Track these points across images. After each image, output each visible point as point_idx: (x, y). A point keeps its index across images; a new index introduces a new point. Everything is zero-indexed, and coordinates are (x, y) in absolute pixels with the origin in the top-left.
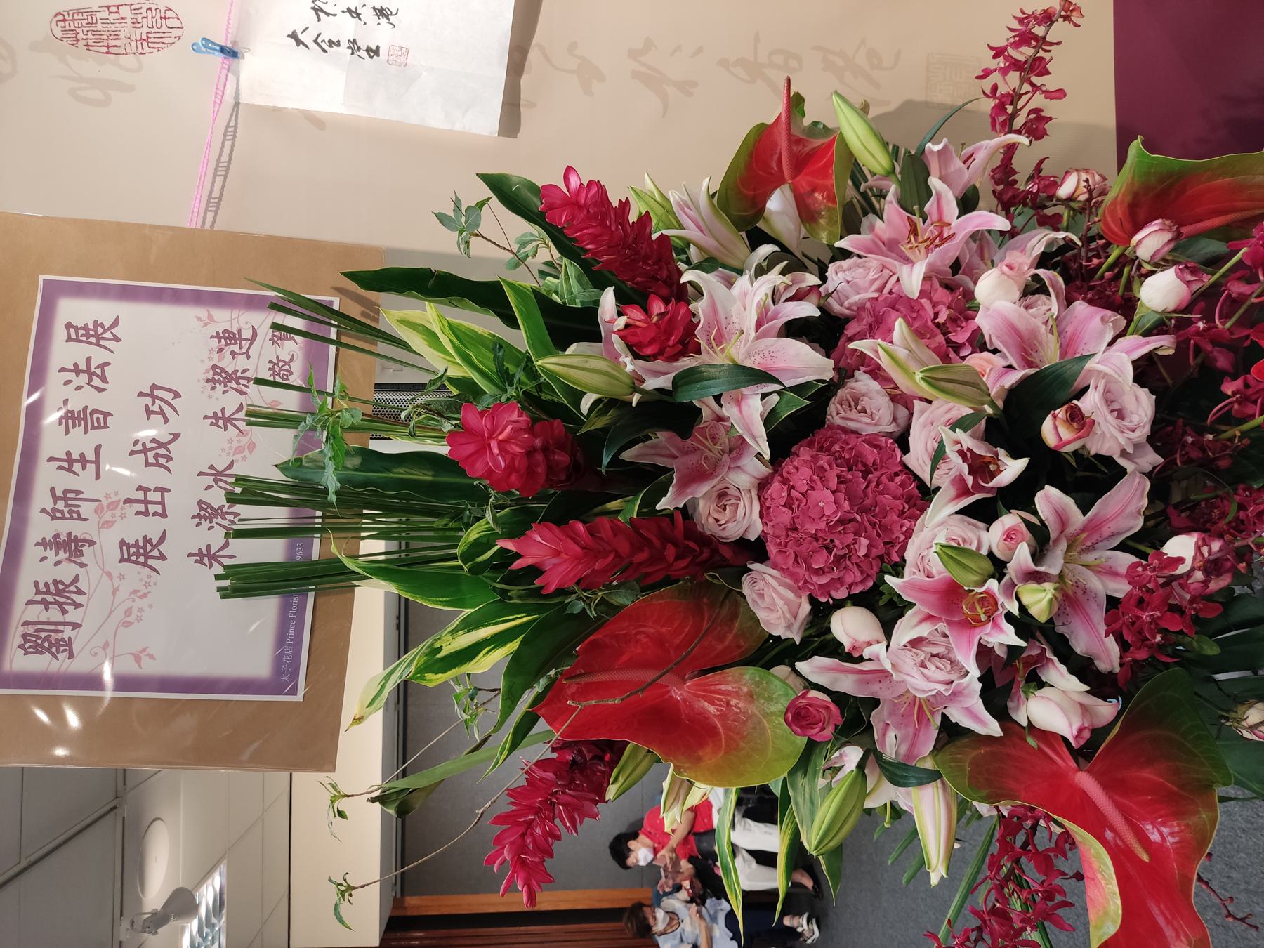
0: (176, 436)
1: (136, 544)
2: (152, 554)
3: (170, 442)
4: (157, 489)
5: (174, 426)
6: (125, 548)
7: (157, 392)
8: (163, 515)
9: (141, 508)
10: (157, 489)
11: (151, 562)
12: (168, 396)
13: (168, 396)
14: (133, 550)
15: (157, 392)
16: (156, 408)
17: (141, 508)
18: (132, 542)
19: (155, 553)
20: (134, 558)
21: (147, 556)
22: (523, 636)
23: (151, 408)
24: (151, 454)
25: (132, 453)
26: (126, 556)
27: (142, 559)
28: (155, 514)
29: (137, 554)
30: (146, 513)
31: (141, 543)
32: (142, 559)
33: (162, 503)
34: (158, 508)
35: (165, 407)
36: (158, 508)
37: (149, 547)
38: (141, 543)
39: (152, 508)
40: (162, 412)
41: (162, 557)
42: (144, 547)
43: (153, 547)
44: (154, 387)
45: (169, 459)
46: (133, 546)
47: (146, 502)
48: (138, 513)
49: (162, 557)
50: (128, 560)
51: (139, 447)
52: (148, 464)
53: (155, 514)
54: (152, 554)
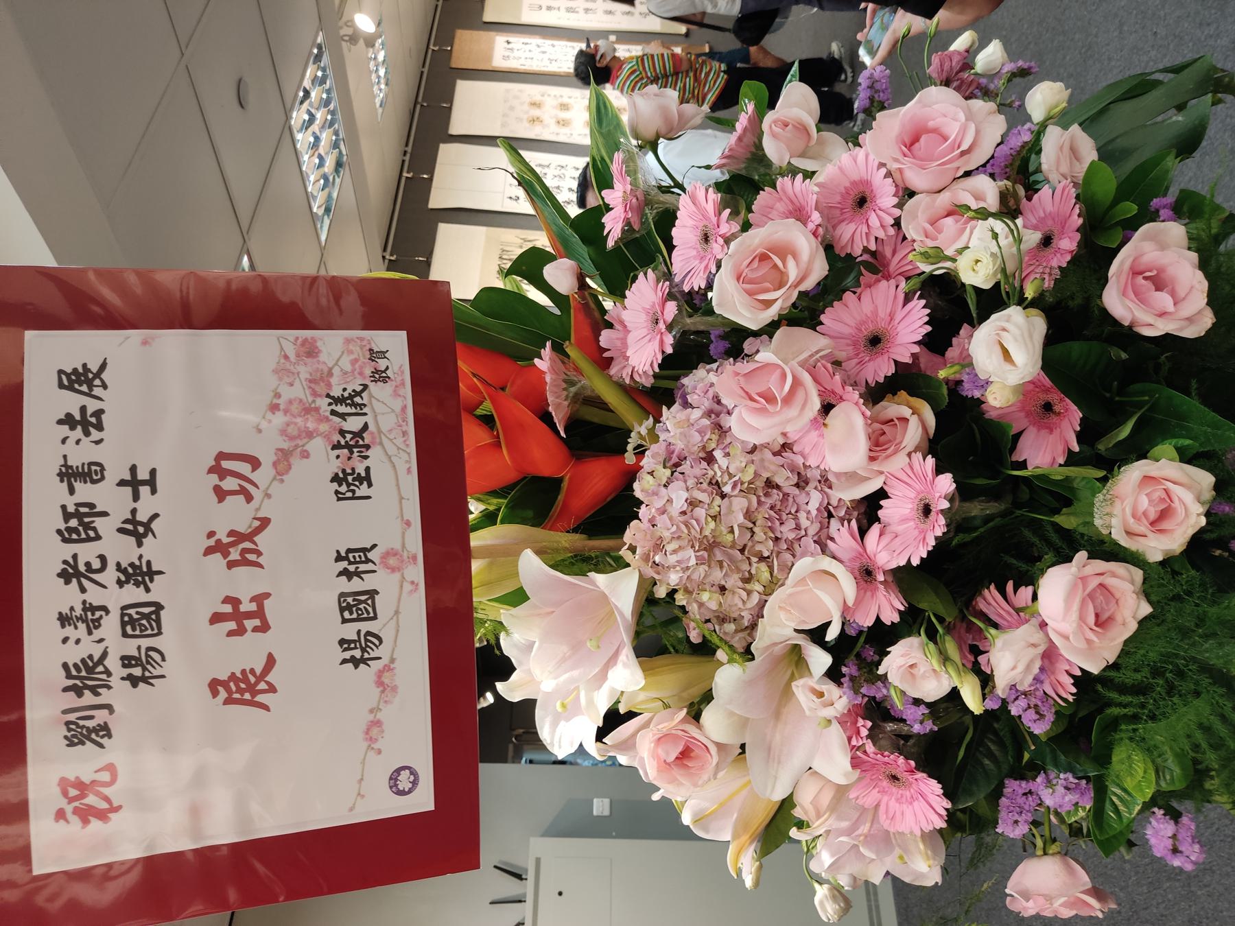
2: (259, 687)
7: (226, 464)
9: (232, 625)
12: (244, 468)
15: (226, 464)
16: (230, 484)
17: (232, 625)
21: (255, 693)
22: (958, 761)
27: (247, 696)
28: (255, 629)
29: (241, 691)
30: (240, 631)
34: (257, 622)
36: (257, 622)
39: (249, 624)
43: (260, 678)
44: (221, 456)
45: (259, 554)
48: (231, 634)
49: (272, 689)
54: (259, 687)
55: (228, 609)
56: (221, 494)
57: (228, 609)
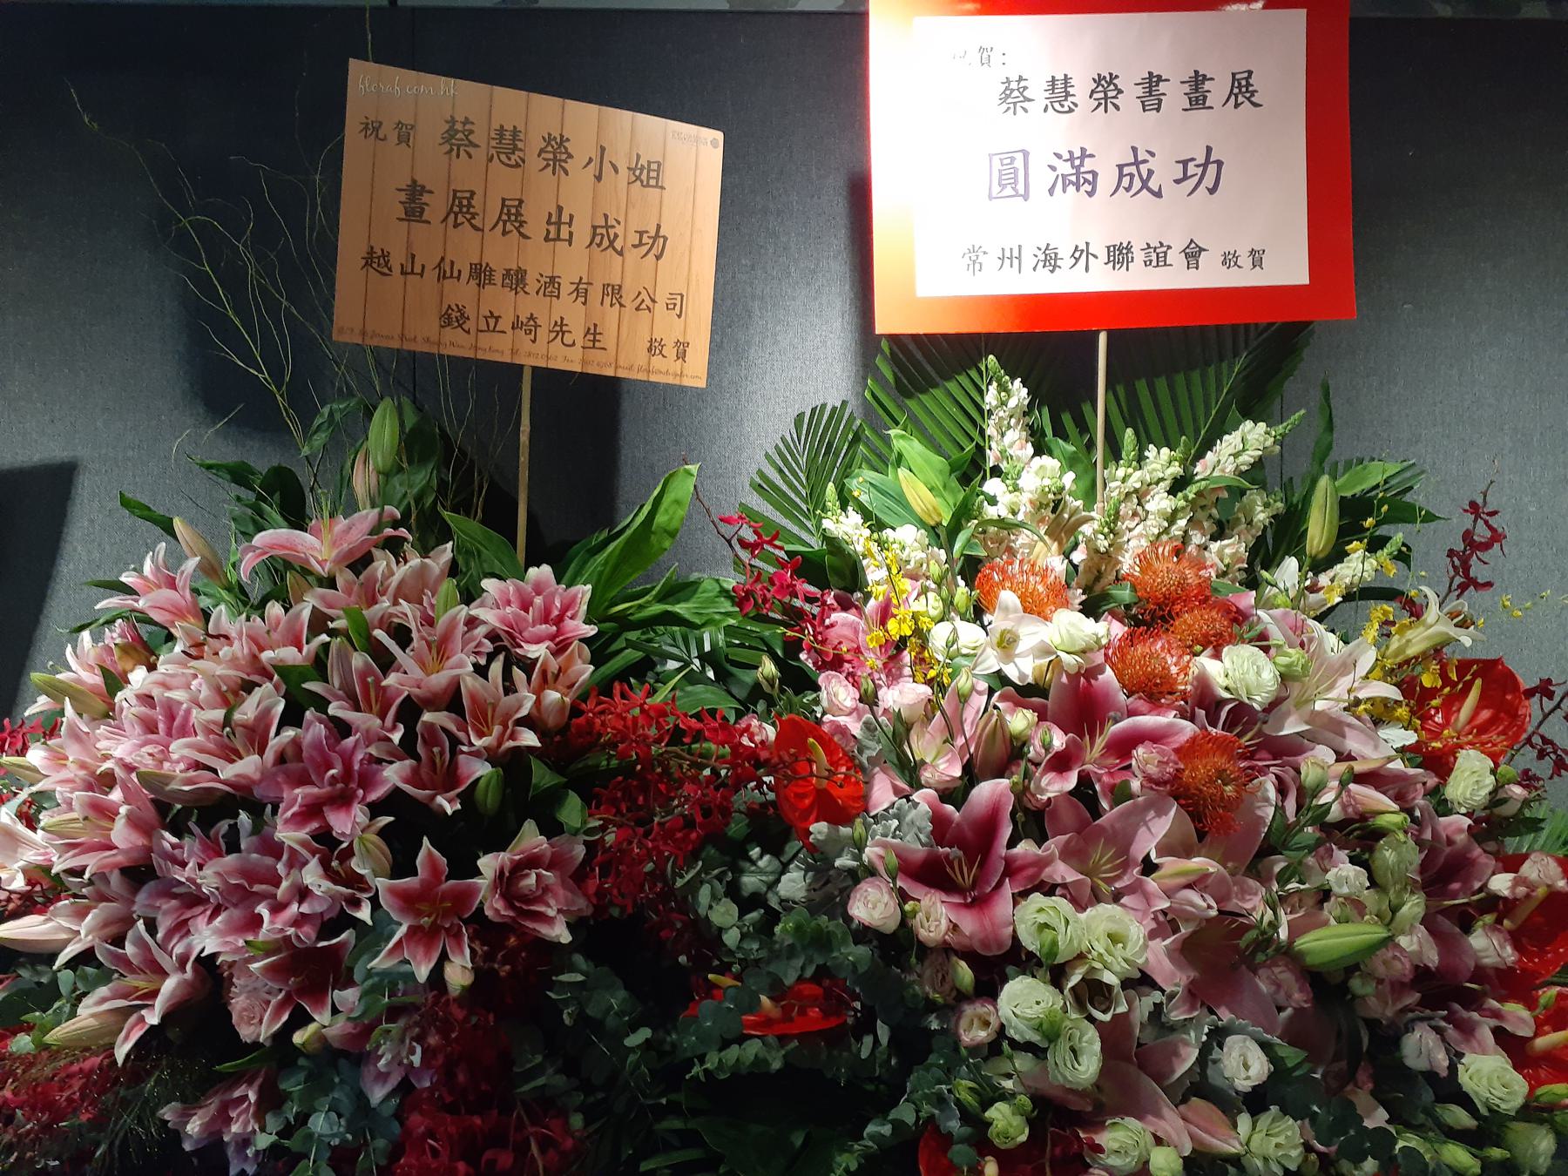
0: (620, 253)
1: (518, 214)
3: (614, 249)
4: (571, 234)
8: (547, 239)
9: (553, 219)
10: (571, 234)
20: (505, 210)
23: (645, 236)
28: (548, 232)
30: (549, 223)
32: (505, 217)
39: (552, 229)
40: (641, 244)
47: (559, 223)
48: (550, 215)
50: (503, 205)
51: (611, 222)
53: (548, 232)
57: (565, 218)
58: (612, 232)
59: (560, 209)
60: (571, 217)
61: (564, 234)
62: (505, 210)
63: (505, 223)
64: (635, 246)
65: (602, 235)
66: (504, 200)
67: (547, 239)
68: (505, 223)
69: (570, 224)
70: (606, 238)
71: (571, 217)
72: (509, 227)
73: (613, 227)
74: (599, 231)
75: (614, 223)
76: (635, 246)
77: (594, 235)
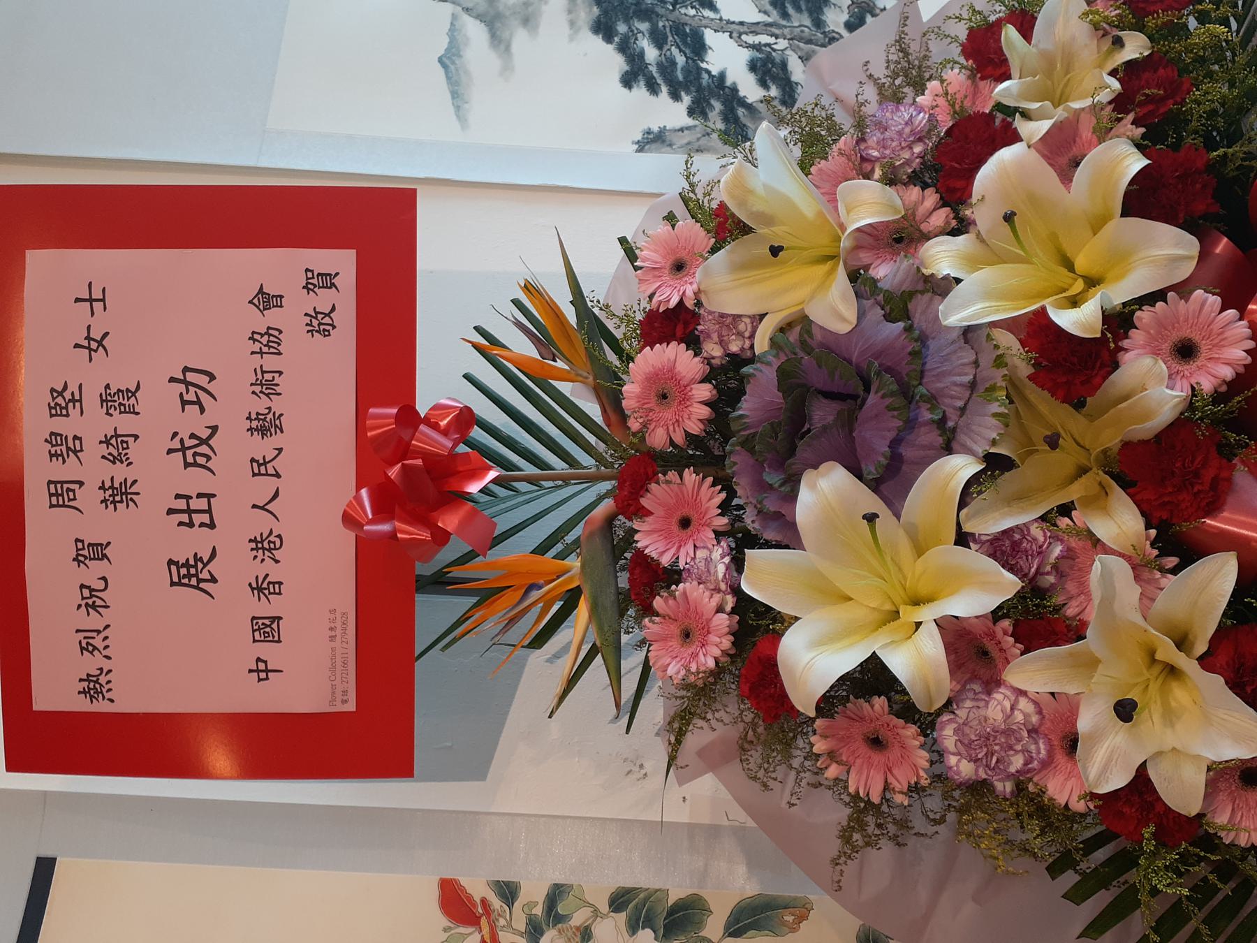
0: (214, 429)
1: (187, 565)
4: (199, 496)
5: (210, 418)
6: (174, 568)
7: (191, 377)
8: (212, 526)
9: (185, 518)
10: (199, 496)
11: (202, 585)
12: (202, 380)
13: (202, 380)
14: (183, 571)
16: (191, 397)
17: (185, 518)
18: (182, 561)
19: (205, 575)
20: (186, 581)
23: (186, 397)
24: (189, 453)
25: (170, 451)
26: (176, 579)
28: (202, 525)
30: (191, 524)
31: (192, 562)
32: (194, 581)
33: (209, 511)
34: (205, 518)
35: (201, 394)
36: (205, 518)
37: (200, 565)
38: (192, 562)
39: (197, 518)
40: (198, 402)
41: (213, 580)
42: (196, 566)
44: (186, 370)
46: (183, 565)
47: (189, 511)
48: (181, 524)
50: (179, 584)
51: (176, 444)
52: (187, 465)
53: (202, 525)
55: (181, 504)
56: (184, 403)
57: (181, 504)
58: (188, 443)
59: (171, 511)
60: (178, 496)
61: (202, 504)
62: (186, 581)
63: (200, 581)
64: (202, 410)
65: (195, 454)
66: (173, 584)
67: (212, 526)
68: (200, 581)
69: (188, 498)
70: (198, 450)
71: (178, 496)
72: (205, 575)
73: (182, 441)
74: (190, 460)
75: (177, 439)
76: (202, 410)
77: (195, 464)
